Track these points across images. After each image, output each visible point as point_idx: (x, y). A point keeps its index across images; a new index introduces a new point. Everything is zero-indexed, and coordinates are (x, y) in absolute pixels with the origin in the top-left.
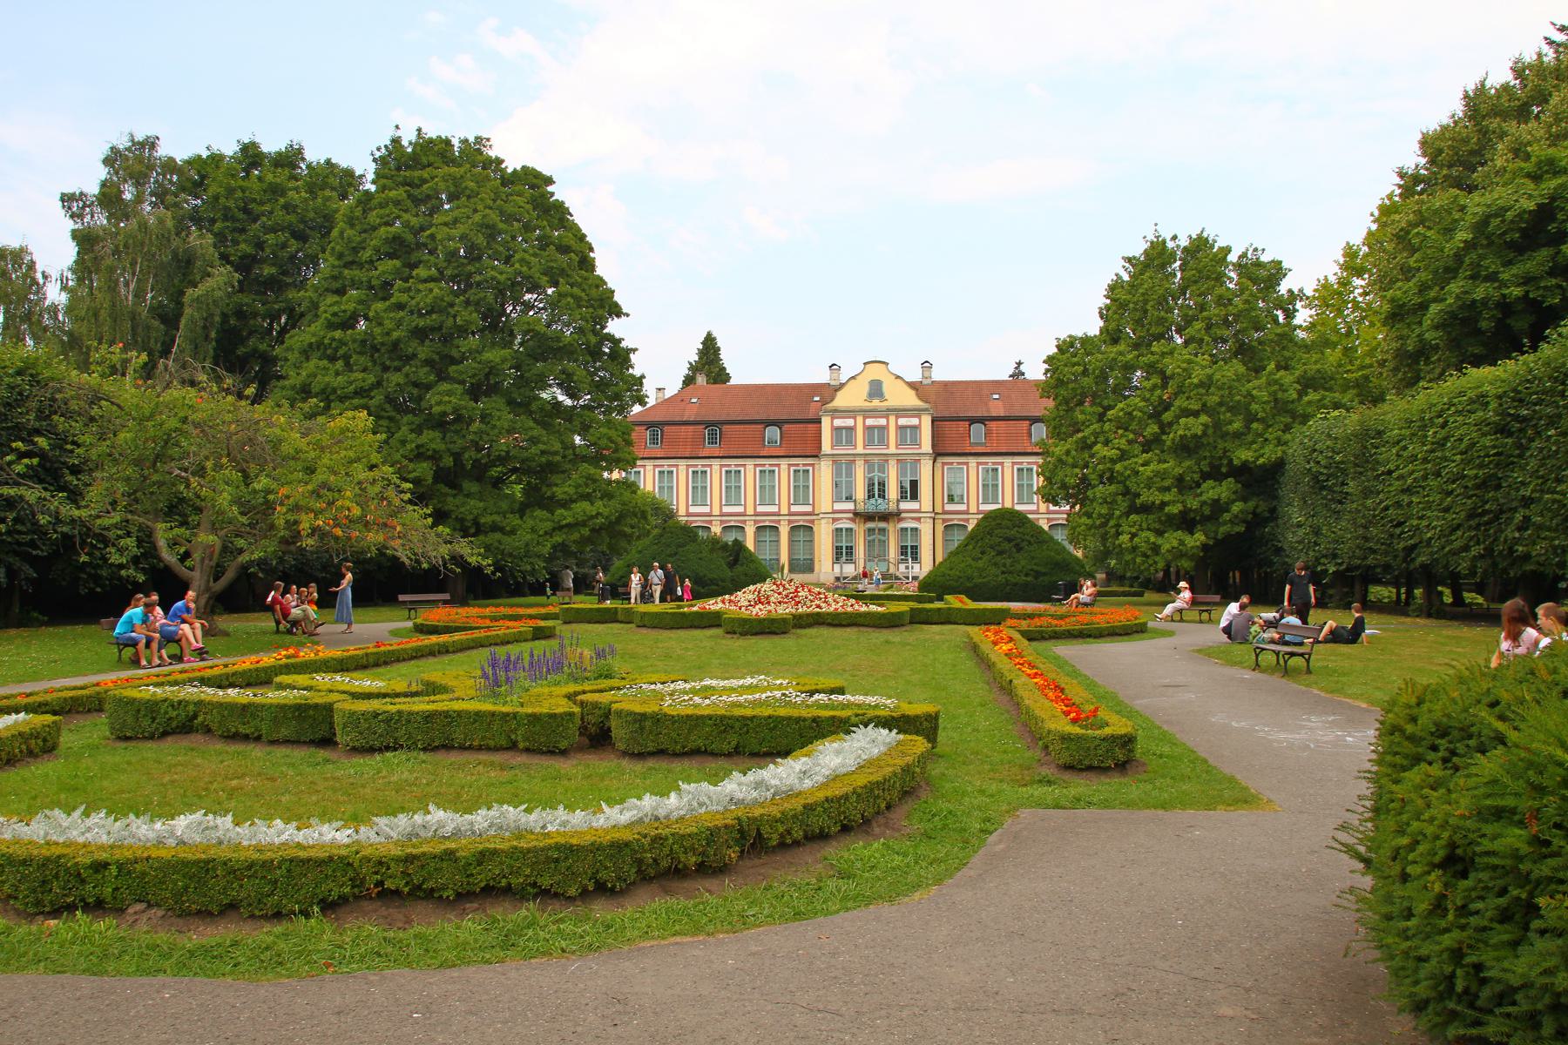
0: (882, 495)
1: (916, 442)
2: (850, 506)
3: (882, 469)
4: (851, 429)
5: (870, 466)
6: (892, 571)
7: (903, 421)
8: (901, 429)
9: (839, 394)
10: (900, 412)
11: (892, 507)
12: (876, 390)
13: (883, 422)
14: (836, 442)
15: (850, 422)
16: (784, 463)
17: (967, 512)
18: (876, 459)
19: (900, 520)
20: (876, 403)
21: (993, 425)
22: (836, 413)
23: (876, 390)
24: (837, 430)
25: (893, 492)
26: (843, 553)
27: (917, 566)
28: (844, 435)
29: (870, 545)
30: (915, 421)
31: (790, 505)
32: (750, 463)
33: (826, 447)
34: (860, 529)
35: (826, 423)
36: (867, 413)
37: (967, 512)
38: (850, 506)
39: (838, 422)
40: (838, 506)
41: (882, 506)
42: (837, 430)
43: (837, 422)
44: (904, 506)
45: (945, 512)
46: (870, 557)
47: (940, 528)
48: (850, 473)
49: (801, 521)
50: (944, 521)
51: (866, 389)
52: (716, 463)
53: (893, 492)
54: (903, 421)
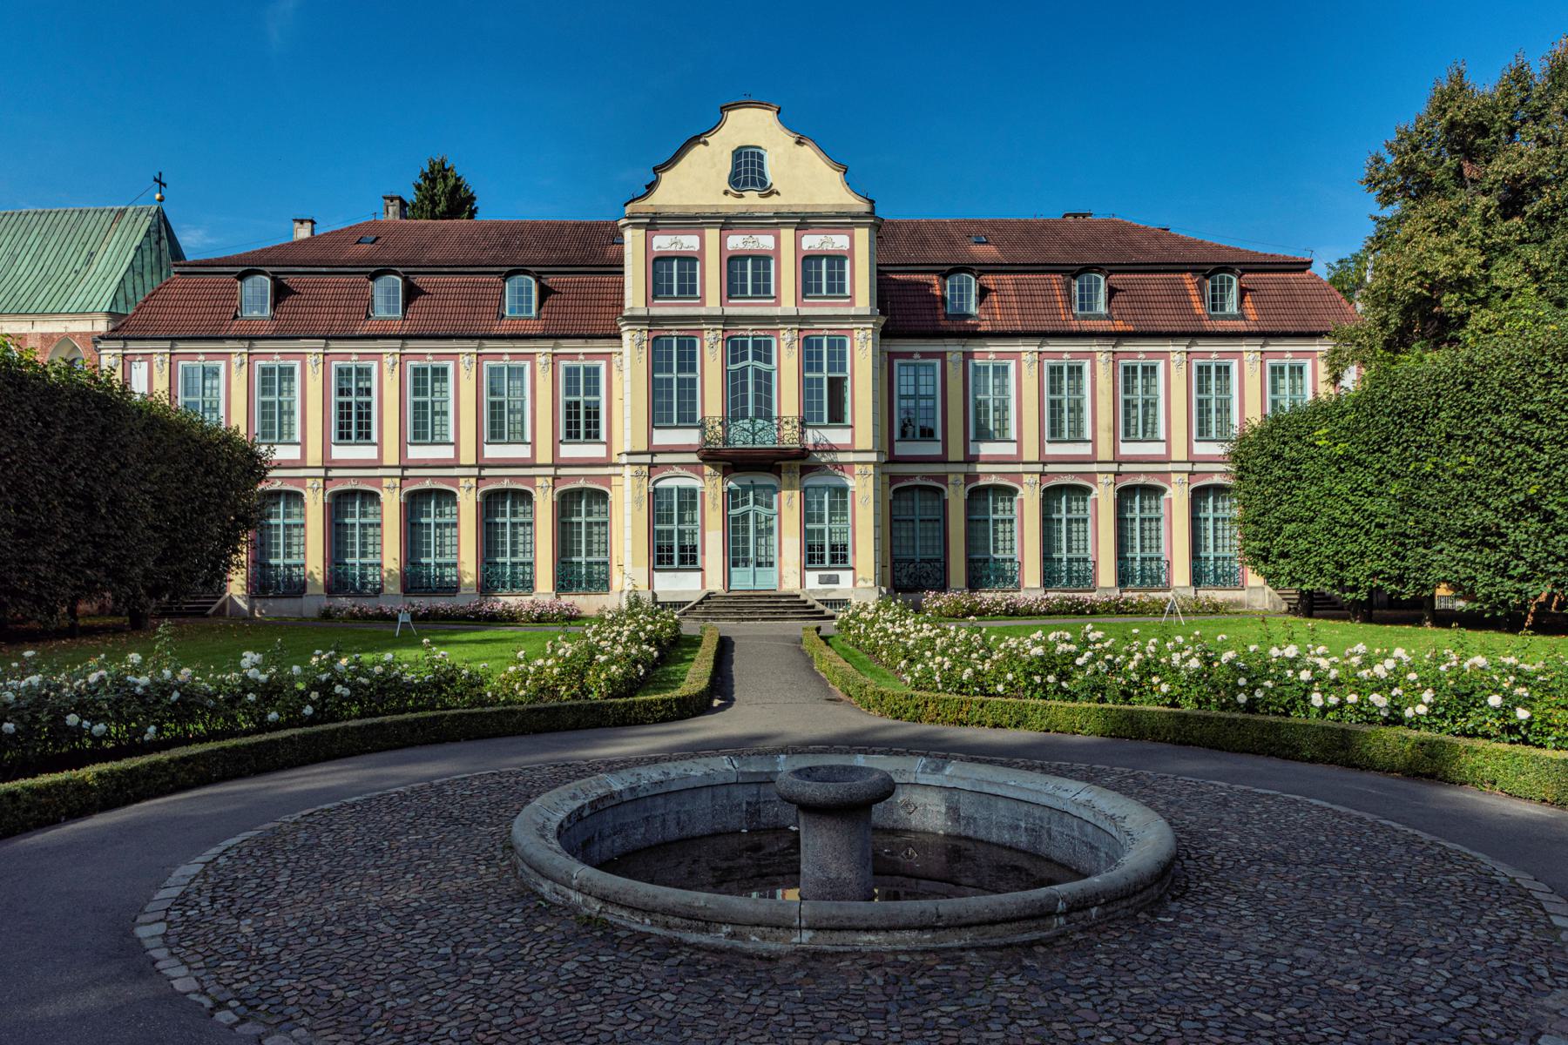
0: (764, 410)
1: (837, 287)
2: (692, 437)
3: (763, 351)
4: (689, 261)
5: (735, 349)
6: (791, 585)
7: (812, 242)
8: (809, 262)
9: (666, 177)
10: (803, 221)
11: (789, 437)
12: (747, 169)
13: (765, 242)
14: (657, 289)
15: (689, 242)
16: (543, 351)
17: (942, 460)
18: (749, 330)
19: (806, 470)
20: (752, 199)
21: (990, 280)
22: (654, 223)
23: (747, 169)
24: (659, 263)
25: (788, 402)
26: (671, 552)
27: (845, 577)
28: (673, 275)
29: (735, 532)
30: (839, 242)
31: (556, 444)
32: (466, 350)
33: (635, 295)
34: (711, 487)
35: (633, 241)
36: (728, 223)
37: (942, 460)
38: (692, 437)
39: (663, 242)
40: (662, 438)
41: (767, 441)
42: (659, 263)
43: (663, 242)
44: (812, 436)
45: (894, 460)
46: (736, 556)
47: (889, 495)
48: (688, 360)
49: (580, 479)
50: (894, 478)
51: (727, 167)
52: (389, 350)
53: (788, 402)
54: (812, 242)
